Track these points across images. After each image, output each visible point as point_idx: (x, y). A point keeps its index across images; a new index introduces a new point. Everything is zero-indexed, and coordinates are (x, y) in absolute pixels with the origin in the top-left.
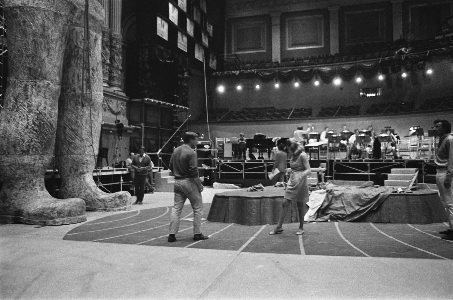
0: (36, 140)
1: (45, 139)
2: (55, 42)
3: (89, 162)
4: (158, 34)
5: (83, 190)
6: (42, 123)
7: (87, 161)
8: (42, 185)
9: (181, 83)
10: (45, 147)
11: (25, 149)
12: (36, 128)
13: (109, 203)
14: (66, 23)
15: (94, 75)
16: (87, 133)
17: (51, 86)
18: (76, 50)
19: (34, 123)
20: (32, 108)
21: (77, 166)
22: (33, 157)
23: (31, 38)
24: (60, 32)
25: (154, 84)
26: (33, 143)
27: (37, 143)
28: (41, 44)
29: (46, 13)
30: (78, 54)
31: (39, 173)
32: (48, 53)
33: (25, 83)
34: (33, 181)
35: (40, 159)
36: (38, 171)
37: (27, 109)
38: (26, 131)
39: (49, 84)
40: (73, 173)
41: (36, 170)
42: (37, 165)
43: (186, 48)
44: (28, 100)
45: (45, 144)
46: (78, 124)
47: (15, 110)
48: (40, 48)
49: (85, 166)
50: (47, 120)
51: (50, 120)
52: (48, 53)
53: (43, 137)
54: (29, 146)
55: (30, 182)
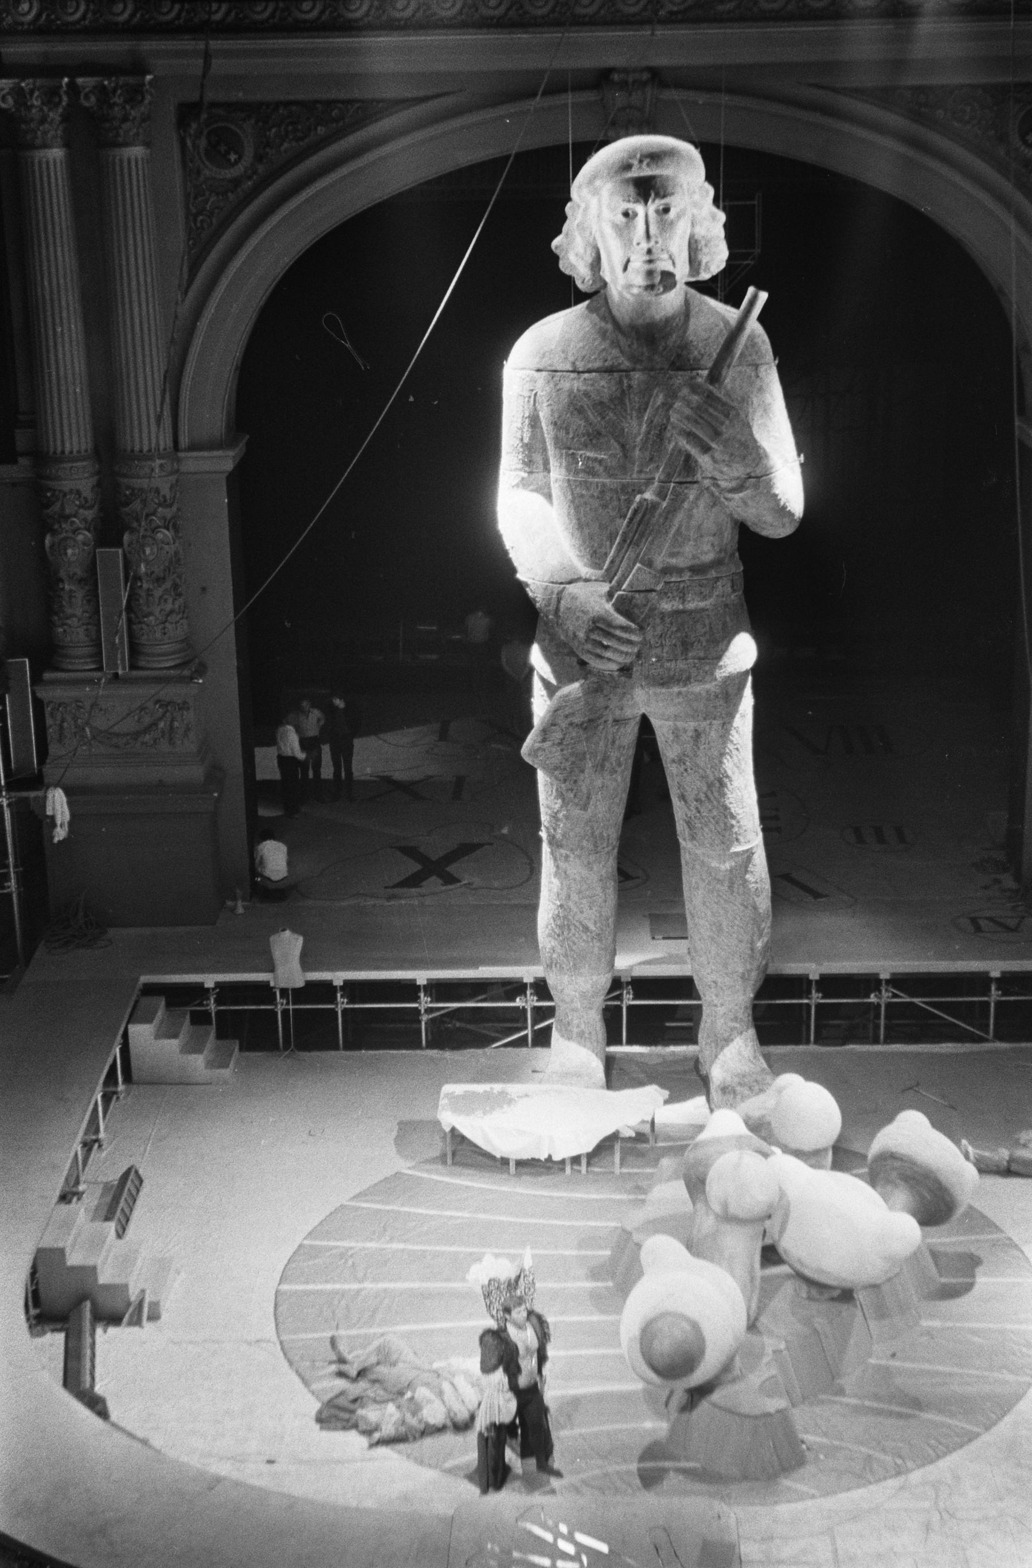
7: (715, 982)
8: (583, 1026)
10: (574, 965)
36: (572, 1001)
39: (567, 857)
41: (567, 999)
42: (566, 991)
54: (551, 958)
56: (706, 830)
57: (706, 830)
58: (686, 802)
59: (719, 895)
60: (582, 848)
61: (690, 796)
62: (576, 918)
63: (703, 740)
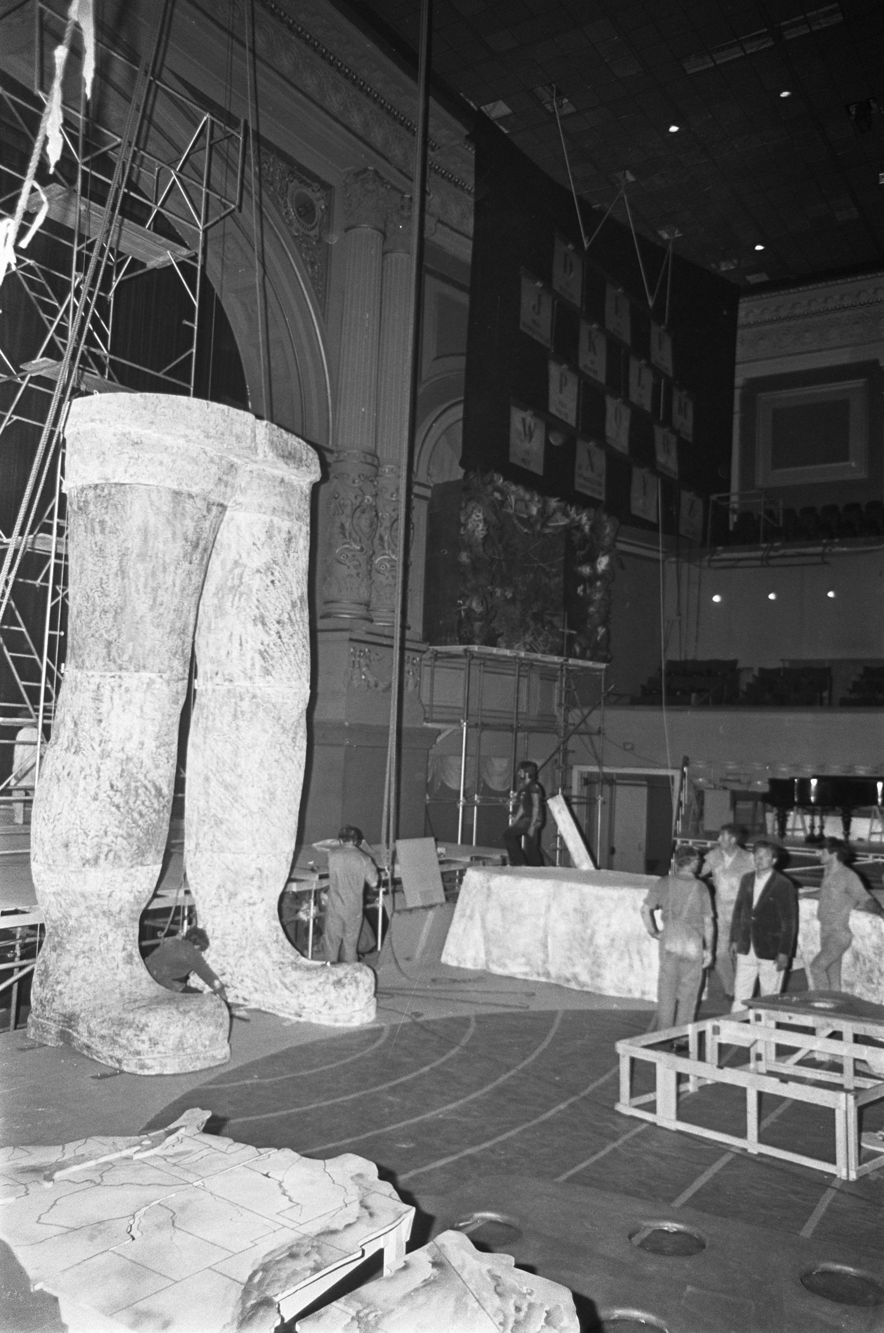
0: (116, 830)
1: (139, 826)
2: (172, 568)
3: (266, 872)
4: (513, 460)
5: (247, 952)
6: (133, 784)
7: (260, 870)
8: (129, 948)
9: (584, 590)
11: (89, 855)
12: (118, 799)
13: (309, 997)
14: (205, 513)
15: (283, 634)
16: (261, 795)
17: (157, 686)
18: (237, 571)
19: (112, 786)
20: (110, 745)
21: (235, 882)
22: (109, 875)
23: (115, 564)
24: (186, 540)
25: (509, 595)
26: (110, 838)
27: (120, 839)
28: (138, 577)
29: (154, 496)
30: (241, 583)
31: (123, 916)
32: (155, 600)
33: (97, 680)
34: (106, 936)
35: (125, 880)
37: (98, 750)
38: (93, 807)
39: (151, 682)
40: (225, 902)
41: (115, 909)
42: (117, 895)
43: (603, 489)
44: (103, 725)
45: (139, 839)
46: (239, 772)
47: (73, 750)
48: (133, 589)
49: (256, 882)
50: (145, 777)
51: (154, 775)
52: (155, 600)
53: (135, 822)
54: (99, 846)
55: (101, 941)
56: (285, 659)
57: (285, 659)
58: (264, 624)
59: (281, 750)
60: (171, 668)
61: (271, 618)
62: (149, 776)
63: (293, 545)
